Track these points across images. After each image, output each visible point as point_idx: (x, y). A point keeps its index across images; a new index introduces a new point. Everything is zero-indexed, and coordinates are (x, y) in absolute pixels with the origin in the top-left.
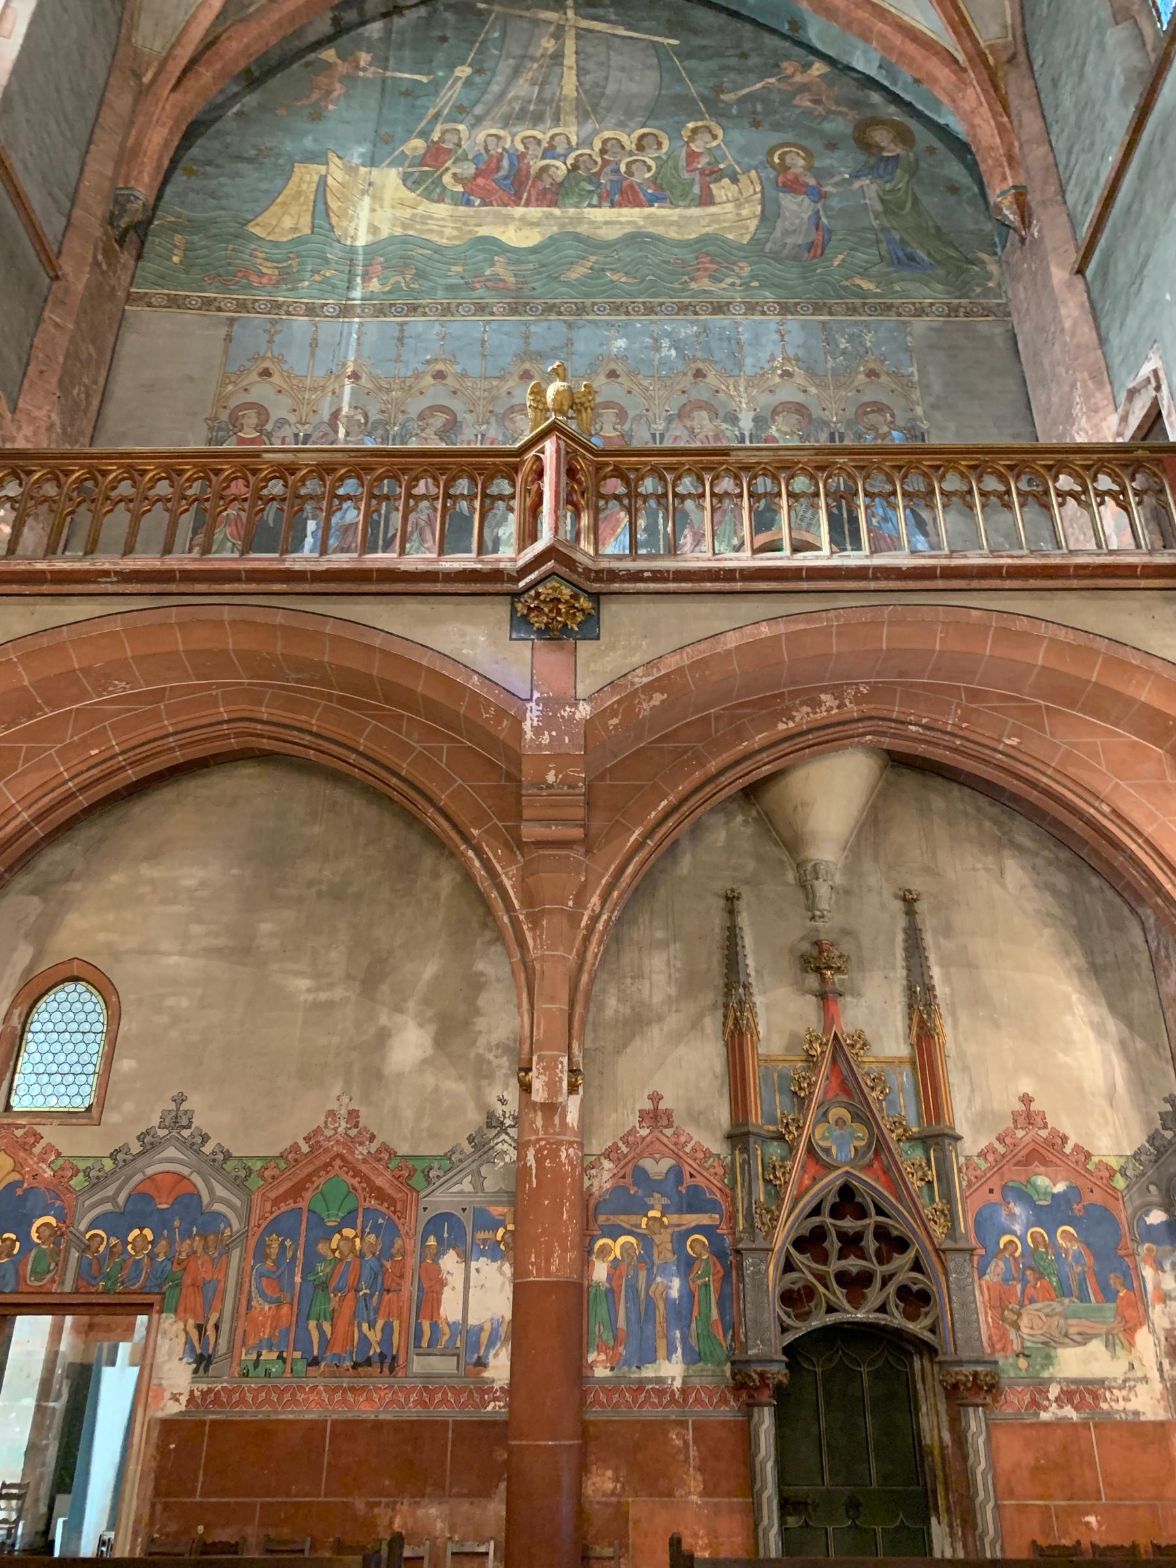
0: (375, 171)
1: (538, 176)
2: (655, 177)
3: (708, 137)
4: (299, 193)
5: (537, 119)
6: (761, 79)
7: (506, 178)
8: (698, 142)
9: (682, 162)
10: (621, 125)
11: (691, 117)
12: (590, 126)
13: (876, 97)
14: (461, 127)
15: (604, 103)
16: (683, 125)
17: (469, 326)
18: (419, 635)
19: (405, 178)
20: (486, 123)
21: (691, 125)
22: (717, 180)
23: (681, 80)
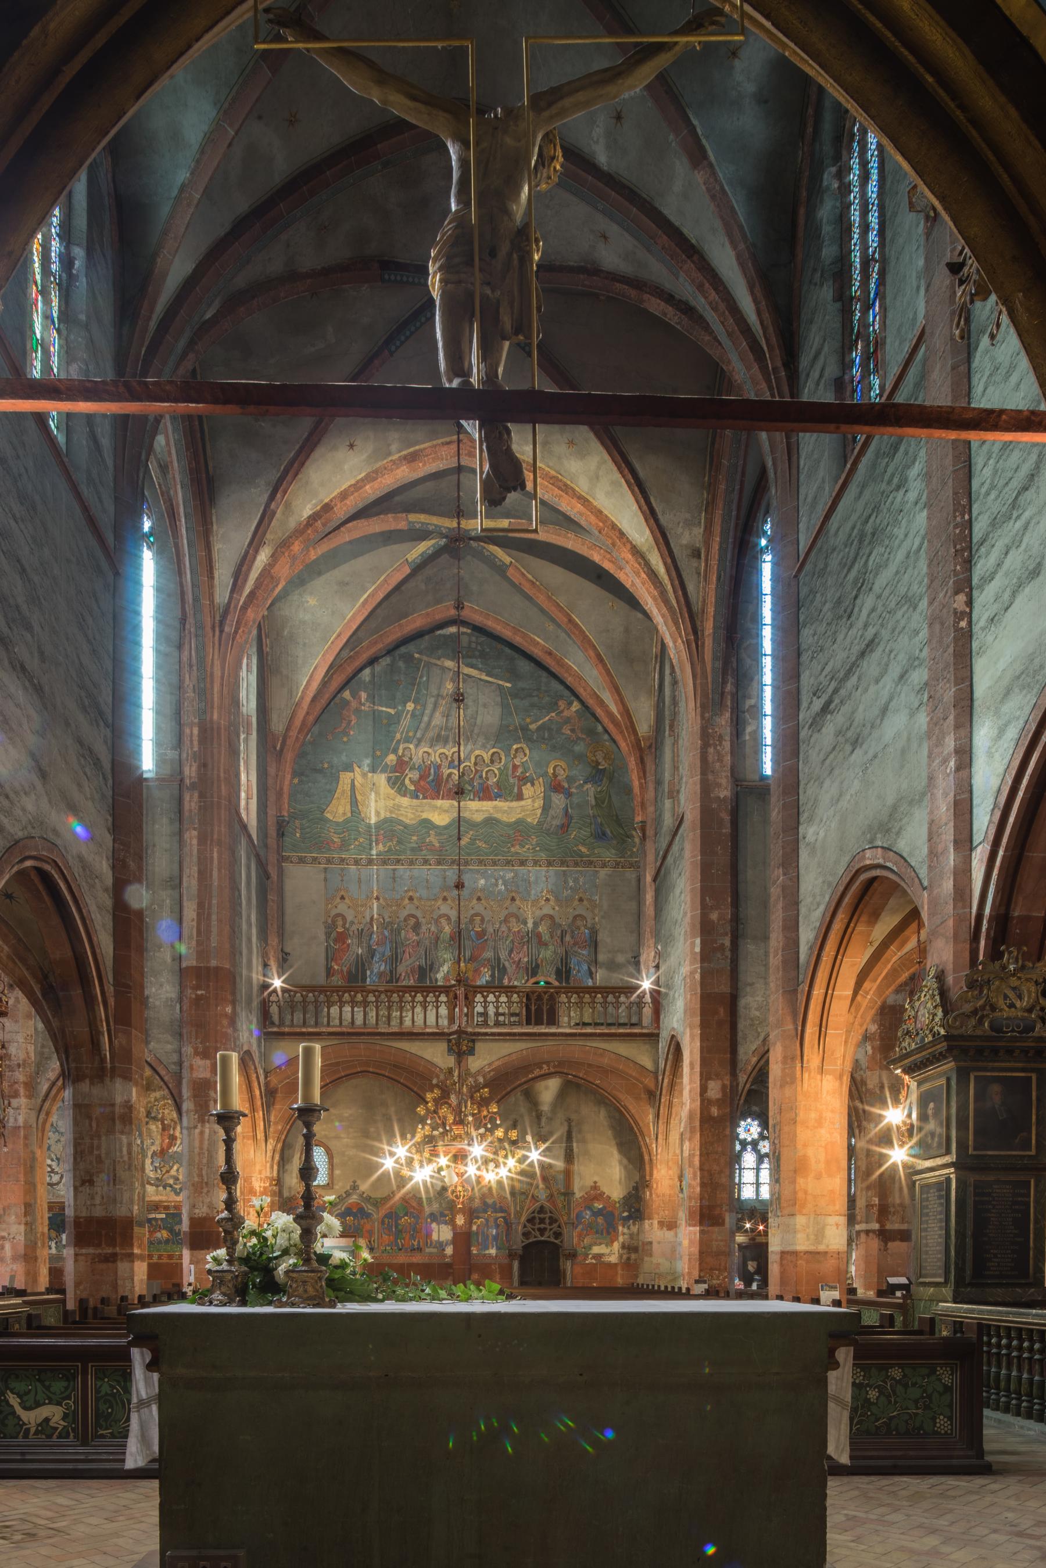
0: (375, 776)
1: (447, 780)
2: (498, 781)
3: (521, 755)
4: (344, 791)
5: (446, 741)
6: (548, 713)
7: (433, 781)
8: (518, 759)
9: (510, 772)
10: (484, 747)
11: (517, 740)
12: (469, 747)
13: (600, 728)
14: (412, 746)
15: (476, 731)
16: (511, 746)
17: (421, 871)
18: (419, 1053)
19: (389, 779)
20: (423, 744)
21: (515, 747)
22: (525, 784)
23: (511, 714)
